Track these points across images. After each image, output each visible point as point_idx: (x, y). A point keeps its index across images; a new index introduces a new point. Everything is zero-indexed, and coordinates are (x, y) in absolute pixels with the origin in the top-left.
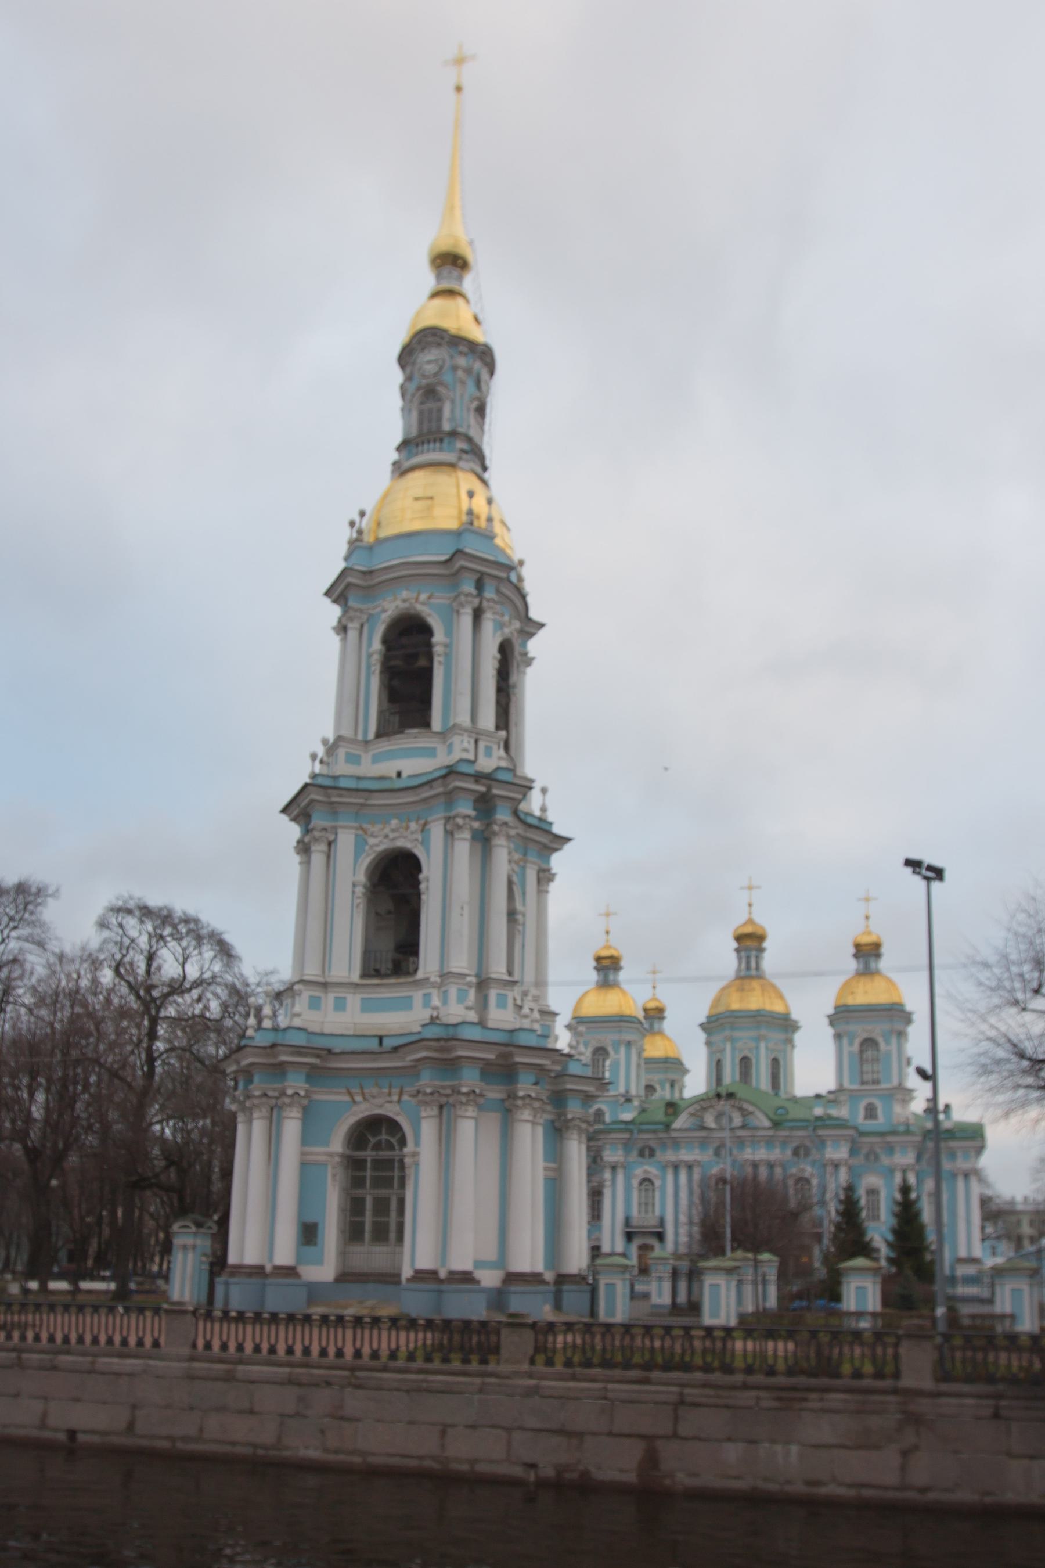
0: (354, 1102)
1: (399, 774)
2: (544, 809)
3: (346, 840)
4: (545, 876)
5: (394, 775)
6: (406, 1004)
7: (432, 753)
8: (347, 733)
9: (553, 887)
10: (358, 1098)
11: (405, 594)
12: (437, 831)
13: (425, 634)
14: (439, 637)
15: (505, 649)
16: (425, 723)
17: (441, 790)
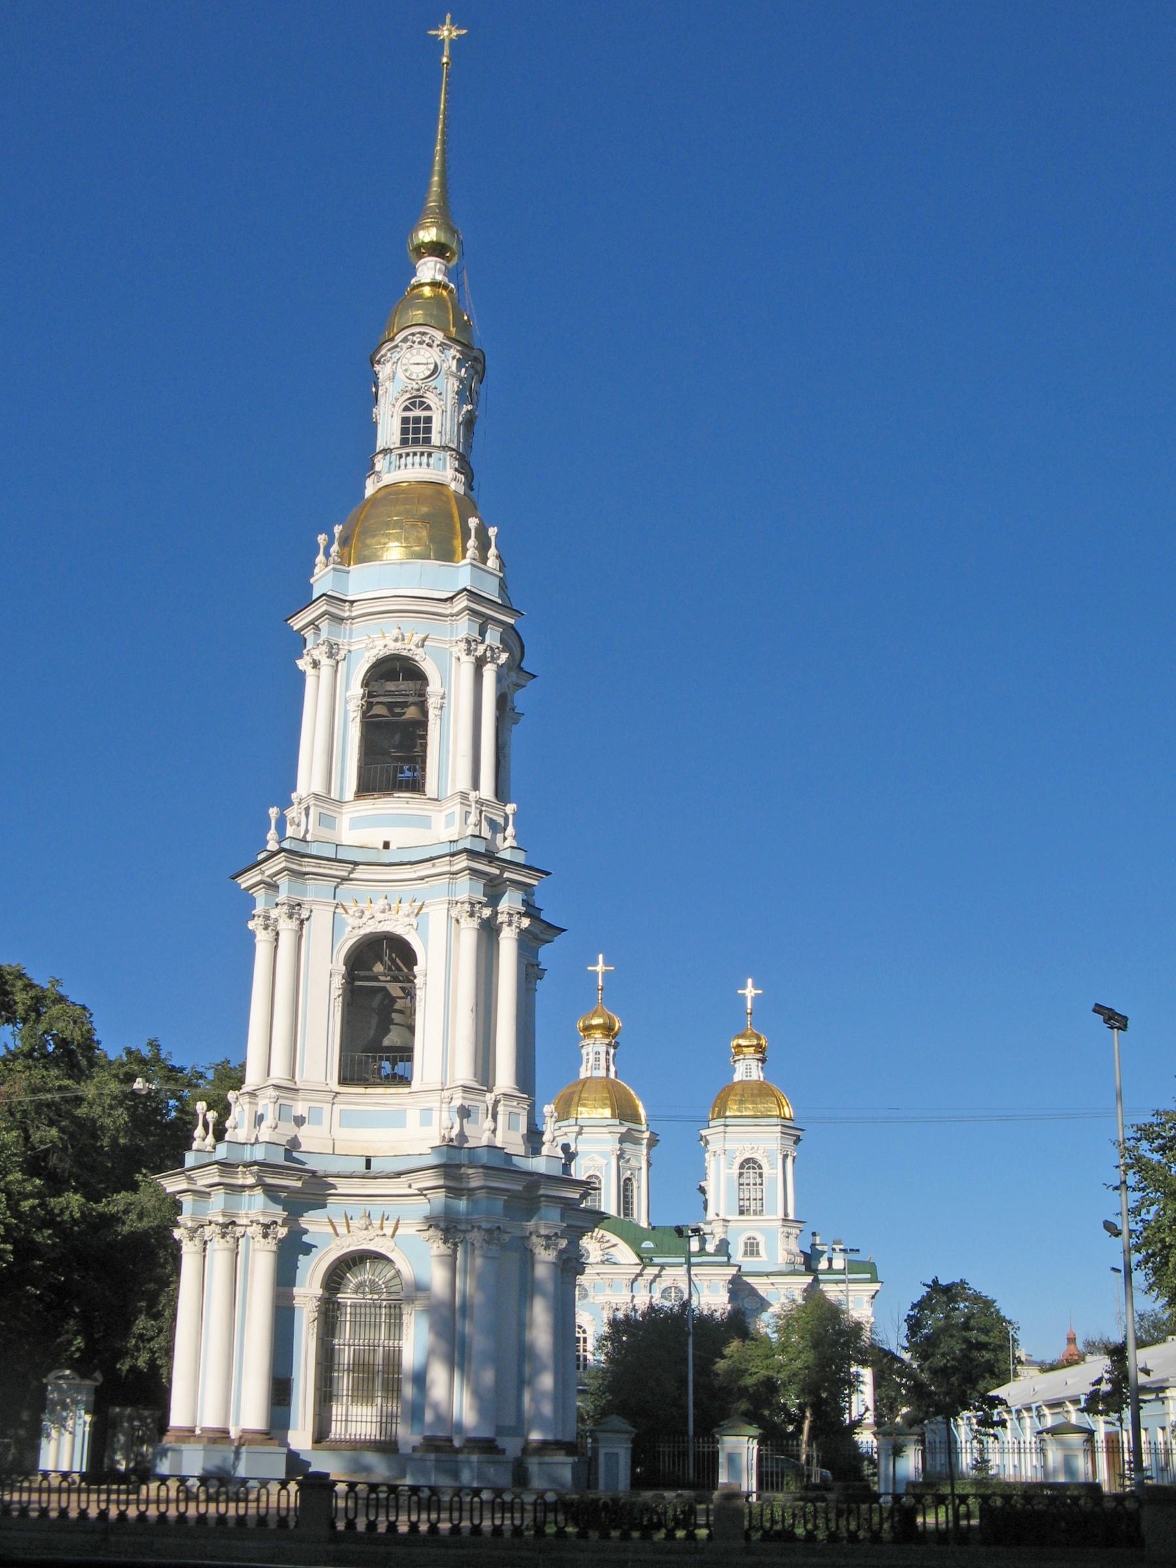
0: (337, 1235)
1: (386, 845)
3: (321, 919)
5: (381, 847)
6: (397, 1120)
7: (424, 822)
10: (342, 1230)
14: (434, 688)
16: (416, 785)
17: (447, 869)
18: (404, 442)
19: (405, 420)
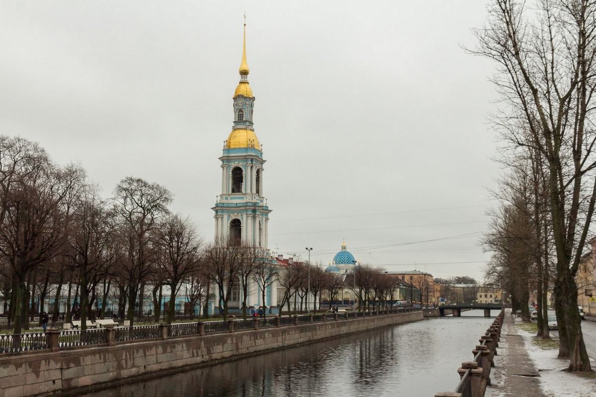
2: (266, 204)
3: (226, 217)
4: (267, 219)
7: (243, 198)
8: (225, 193)
9: (269, 221)
11: (236, 162)
12: (245, 216)
13: (241, 170)
15: (258, 172)
18: (239, 119)
19: (239, 115)
